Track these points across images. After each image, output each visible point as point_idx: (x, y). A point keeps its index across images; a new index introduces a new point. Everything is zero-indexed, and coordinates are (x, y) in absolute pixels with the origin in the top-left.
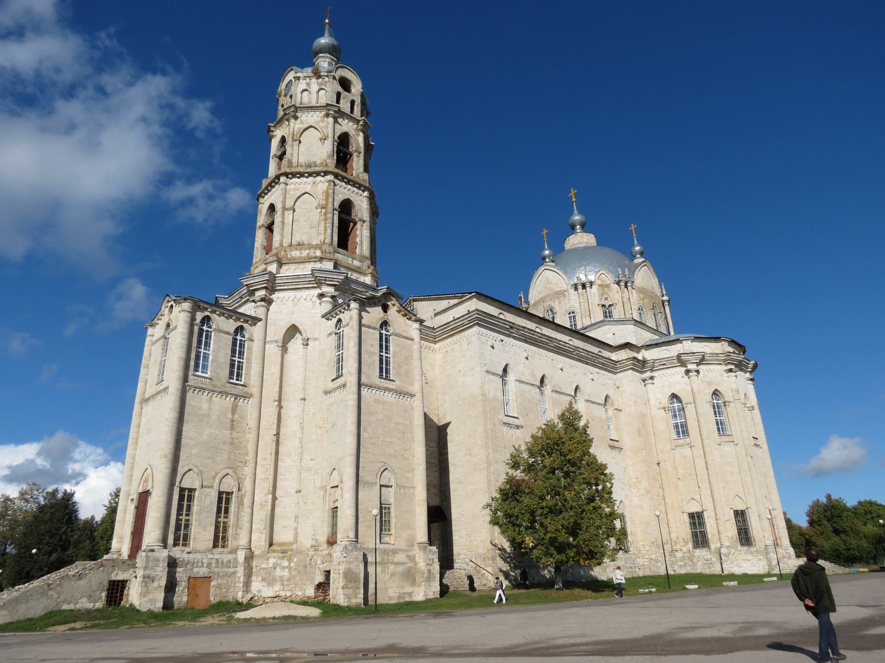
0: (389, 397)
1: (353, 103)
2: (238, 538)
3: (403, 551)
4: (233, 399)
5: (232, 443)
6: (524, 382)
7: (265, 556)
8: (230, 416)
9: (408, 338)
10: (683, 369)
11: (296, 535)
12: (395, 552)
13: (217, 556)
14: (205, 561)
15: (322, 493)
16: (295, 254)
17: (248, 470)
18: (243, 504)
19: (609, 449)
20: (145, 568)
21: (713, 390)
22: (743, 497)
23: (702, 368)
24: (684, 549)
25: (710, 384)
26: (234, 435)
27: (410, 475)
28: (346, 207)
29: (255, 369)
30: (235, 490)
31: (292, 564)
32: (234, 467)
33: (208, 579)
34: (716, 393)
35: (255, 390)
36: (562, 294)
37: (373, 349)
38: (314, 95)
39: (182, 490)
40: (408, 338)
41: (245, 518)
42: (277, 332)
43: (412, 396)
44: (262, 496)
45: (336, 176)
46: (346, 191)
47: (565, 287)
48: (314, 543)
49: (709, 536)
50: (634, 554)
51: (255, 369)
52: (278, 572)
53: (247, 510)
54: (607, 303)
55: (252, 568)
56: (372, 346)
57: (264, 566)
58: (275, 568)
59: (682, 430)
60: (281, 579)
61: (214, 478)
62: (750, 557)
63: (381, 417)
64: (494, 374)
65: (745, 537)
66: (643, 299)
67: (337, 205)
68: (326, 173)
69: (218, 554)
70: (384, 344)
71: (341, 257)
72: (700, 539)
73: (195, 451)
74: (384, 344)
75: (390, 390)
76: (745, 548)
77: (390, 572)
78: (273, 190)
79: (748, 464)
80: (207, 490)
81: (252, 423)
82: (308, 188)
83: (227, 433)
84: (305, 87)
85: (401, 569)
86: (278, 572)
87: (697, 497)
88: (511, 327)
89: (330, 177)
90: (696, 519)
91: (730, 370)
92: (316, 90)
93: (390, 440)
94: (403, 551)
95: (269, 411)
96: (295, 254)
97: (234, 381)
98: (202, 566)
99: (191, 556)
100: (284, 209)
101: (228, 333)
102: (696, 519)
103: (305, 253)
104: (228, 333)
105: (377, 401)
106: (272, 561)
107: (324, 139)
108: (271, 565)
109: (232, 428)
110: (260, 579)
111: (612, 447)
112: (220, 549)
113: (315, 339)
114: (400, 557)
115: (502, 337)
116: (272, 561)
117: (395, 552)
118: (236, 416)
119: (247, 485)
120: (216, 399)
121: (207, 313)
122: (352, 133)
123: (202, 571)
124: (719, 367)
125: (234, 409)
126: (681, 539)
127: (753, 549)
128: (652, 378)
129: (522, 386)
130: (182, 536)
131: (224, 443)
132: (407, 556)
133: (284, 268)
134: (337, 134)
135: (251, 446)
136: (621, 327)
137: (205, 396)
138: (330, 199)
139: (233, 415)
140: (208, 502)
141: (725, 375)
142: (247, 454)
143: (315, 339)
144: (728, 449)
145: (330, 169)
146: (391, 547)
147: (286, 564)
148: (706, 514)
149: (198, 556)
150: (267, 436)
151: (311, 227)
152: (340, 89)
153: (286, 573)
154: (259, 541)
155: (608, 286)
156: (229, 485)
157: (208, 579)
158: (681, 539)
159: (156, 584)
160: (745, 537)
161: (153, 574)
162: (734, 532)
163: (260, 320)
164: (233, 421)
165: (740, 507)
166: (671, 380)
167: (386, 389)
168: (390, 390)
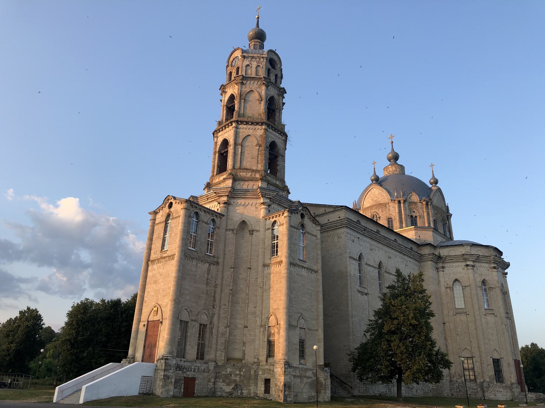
0: (304, 272)
1: (276, 76)
2: (210, 355)
4: (208, 265)
5: (207, 293)
7: (224, 366)
8: (206, 276)
11: (244, 354)
13: (199, 365)
14: (193, 367)
15: (262, 330)
18: (212, 333)
20: (165, 370)
22: (499, 351)
23: (477, 264)
24: (459, 381)
25: (481, 275)
26: (208, 288)
27: (314, 322)
30: (208, 323)
31: (242, 373)
33: (194, 379)
34: (484, 282)
35: (221, 261)
36: (383, 206)
41: (214, 342)
43: (316, 272)
45: (268, 125)
48: (256, 360)
51: (221, 246)
52: (233, 377)
53: (215, 337)
56: (296, 240)
57: (224, 373)
58: (231, 375)
60: (235, 380)
61: (197, 315)
62: (502, 390)
66: (436, 214)
69: (198, 364)
73: (188, 298)
76: (499, 384)
77: (304, 382)
78: (227, 129)
80: (194, 323)
82: (251, 132)
83: (204, 286)
84: (248, 64)
85: (310, 380)
86: (233, 377)
87: (469, 348)
88: (365, 230)
92: (255, 66)
93: (304, 299)
94: (311, 370)
95: (228, 273)
97: (208, 254)
98: (191, 371)
99: (186, 364)
100: (236, 144)
103: (249, 175)
105: (298, 274)
108: (228, 372)
109: (207, 284)
110: (221, 381)
113: (257, 231)
114: (309, 374)
115: (358, 235)
116: (229, 370)
118: (209, 276)
121: (196, 211)
122: (276, 97)
123: (190, 374)
124: (487, 265)
126: (457, 374)
127: (504, 385)
128: (443, 267)
132: (313, 373)
134: (268, 97)
139: (208, 275)
140: (194, 330)
142: (214, 301)
143: (257, 231)
146: (305, 367)
147: (238, 372)
149: (189, 364)
151: (252, 158)
152: (270, 67)
153: (238, 378)
154: (221, 357)
156: (204, 319)
157: (194, 379)
158: (457, 374)
159: (169, 381)
162: (492, 373)
163: (223, 215)
164: (207, 279)
165: (496, 357)
168: (305, 268)
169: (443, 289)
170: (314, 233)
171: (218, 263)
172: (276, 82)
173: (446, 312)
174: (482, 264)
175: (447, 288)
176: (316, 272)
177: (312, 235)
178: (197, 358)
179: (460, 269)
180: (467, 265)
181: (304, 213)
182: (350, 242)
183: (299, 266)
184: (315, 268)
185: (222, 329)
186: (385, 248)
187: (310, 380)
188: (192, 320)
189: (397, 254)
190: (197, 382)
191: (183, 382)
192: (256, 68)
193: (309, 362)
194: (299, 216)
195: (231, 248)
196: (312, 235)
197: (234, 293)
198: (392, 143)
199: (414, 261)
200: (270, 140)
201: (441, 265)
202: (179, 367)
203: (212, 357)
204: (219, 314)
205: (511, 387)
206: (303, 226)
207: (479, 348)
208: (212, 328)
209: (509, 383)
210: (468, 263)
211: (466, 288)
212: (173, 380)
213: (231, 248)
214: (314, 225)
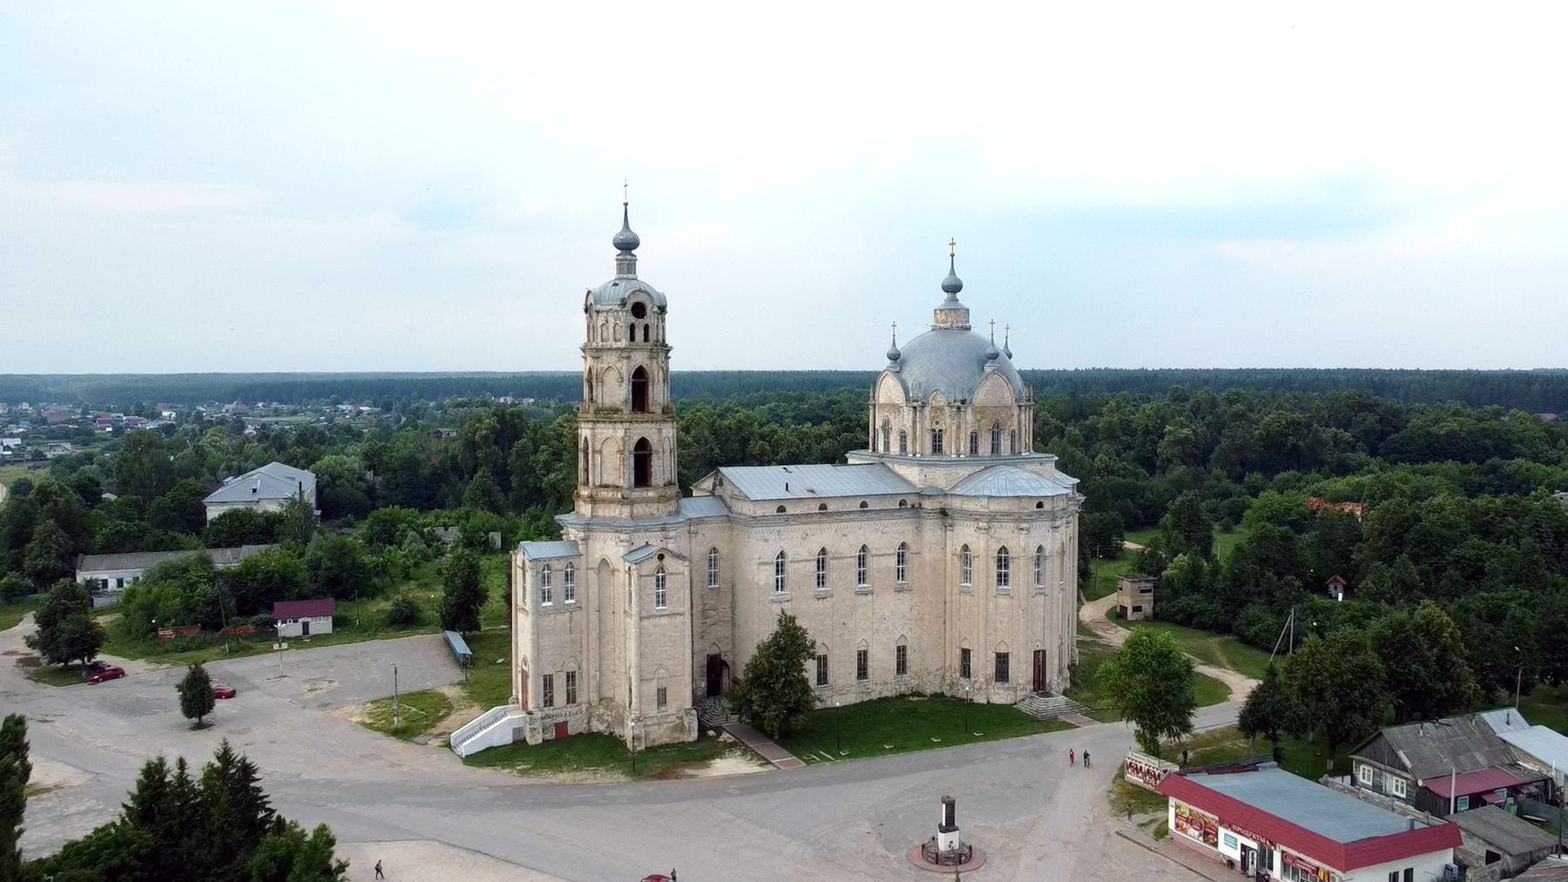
1: (646, 328)
2: (582, 698)
17: (584, 656)
25: (999, 540)
28: (643, 444)
29: (583, 590)
51: (583, 590)
54: (938, 428)
59: (967, 576)
65: (1002, 673)
67: (632, 448)
70: (661, 582)
71: (639, 493)
72: (966, 671)
74: (661, 582)
90: (966, 654)
95: (594, 617)
102: (966, 654)
119: (584, 666)
123: (561, 720)
125: (571, 619)
130: (549, 702)
144: (1003, 601)
150: (594, 635)
152: (633, 319)
154: (594, 697)
155: (941, 409)
156: (572, 667)
160: (1002, 673)
166: (966, 533)
169: (949, 556)
179: (971, 530)
185: (592, 672)
195: (594, 588)
197: (600, 637)
200: (636, 439)
205: (1015, 690)
206: (661, 569)
213: (594, 588)
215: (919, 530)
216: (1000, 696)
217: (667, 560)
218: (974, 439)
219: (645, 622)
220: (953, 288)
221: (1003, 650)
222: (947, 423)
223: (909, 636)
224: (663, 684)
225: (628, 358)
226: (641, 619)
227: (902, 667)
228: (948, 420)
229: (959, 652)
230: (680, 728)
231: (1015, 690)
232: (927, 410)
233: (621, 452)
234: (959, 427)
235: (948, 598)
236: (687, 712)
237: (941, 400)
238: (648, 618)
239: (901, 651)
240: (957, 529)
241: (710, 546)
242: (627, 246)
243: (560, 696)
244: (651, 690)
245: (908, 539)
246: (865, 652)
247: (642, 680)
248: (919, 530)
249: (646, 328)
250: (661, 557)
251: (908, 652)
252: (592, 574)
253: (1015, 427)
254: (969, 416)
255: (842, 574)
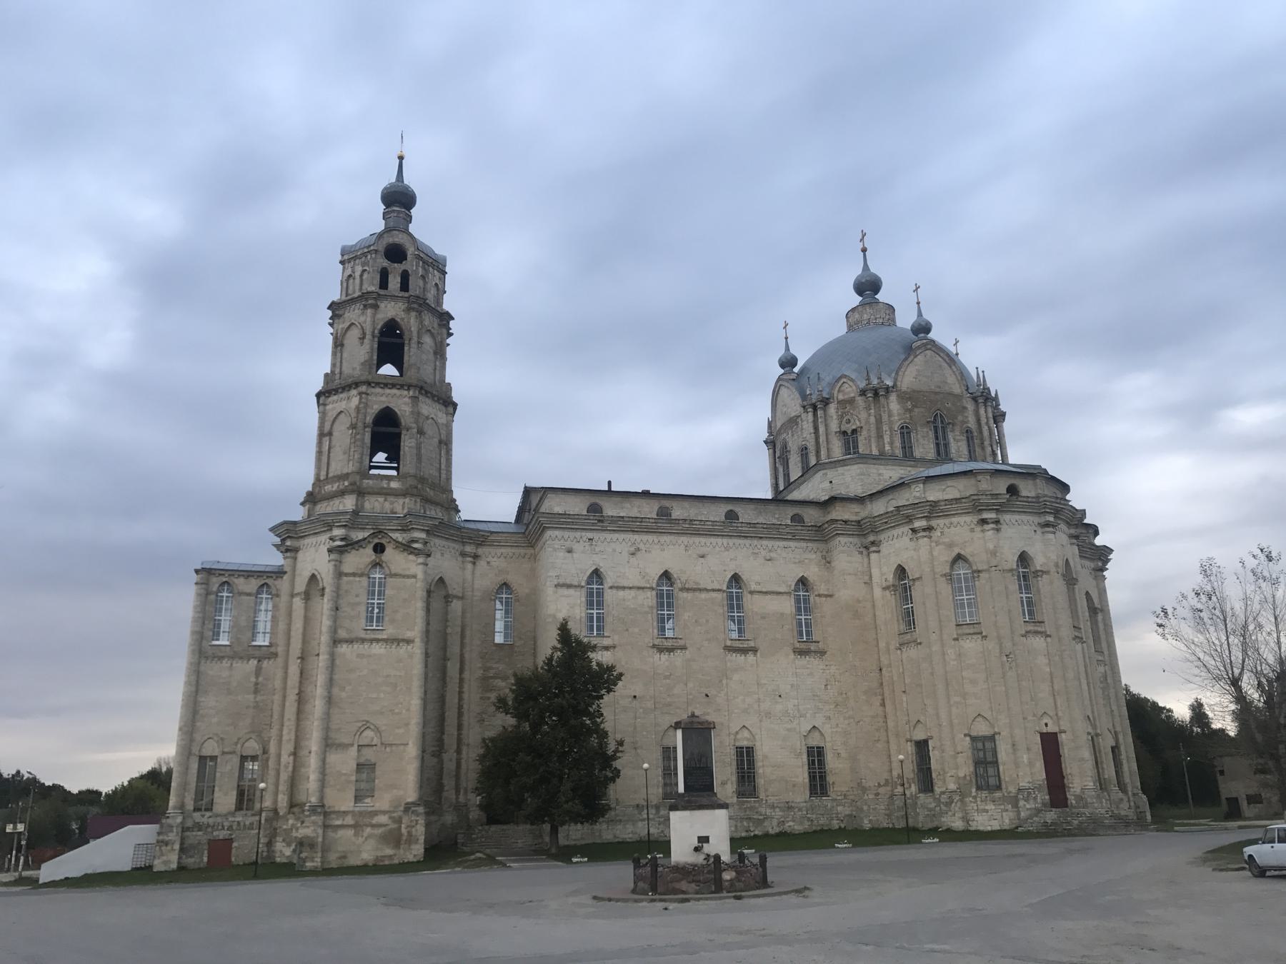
0: (378, 649)
1: (405, 277)
3: (384, 812)
6: (624, 588)
8: (253, 679)
9: (408, 577)
10: (906, 529)
12: (376, 813)
13: (240, 819)
14: (226, 824)
16: (328, 488)
17: (274, 732)
19: (792, 656)
21: (954, 554)
25: (950, 546)
27: (401, 731)
32: (258, 732)
33: (229, 841)
35: (280, 650)
36: (793, 422)
37: (357, 600)
38: (358, 281)
39: (202, 759)
40: (408, 577)
42: (301, 586)
43: (408, 641)
44: (286, 759)
46: (383, 399)
47: (797, 413)
49: (934, 775)
50: (834, 800)
54: (849, 428)
55: (275, 829)
59: (909, 618)
61: (236, 744)
62: (990, 807)
63: (365, 672)
64: (569, 586)
66: (910, 411)
67: (369, 419)
68: (357, 384)
72: (926, 780)
73: (215, 720)
75: (378, 640)
77: (365, 834)
79: (1003, 665)
81: (278, 684)
82: (342, 405)
83: (251, 697)
85: (381, 830)
89: (363, 388)
91: (984, 522)
94: (384, 812)
95: (294, 669)
96: (328, 488)
101: (249, 594)
104: (249, 594)
105: (360, 656)
106: (291, 822)
107: (362, 338)
109: (256, 692)
111: (801, 653)
112: (243, 812)
114: (383, 819)
115: (590, 535)
117: (376, 813)
118: (260, 679)
120: (238, 665)
123: (222, 834)
124: (968, 519)
125: (258, 672)
127: (998, 794)
129: (621, 593)
131: (248, 707)
133: (318, 507)
135: (276, 708)
136: (840, 470)
137: (226, 663)
138: (360, 416)
139: (257, 675)
140: (229, 767)
141: (978, 529)
145: (363, 378)
148: (931, 743)
149: (219, 820)
152: (386, 263)
154: (283, 801)
155: (851, 401)
157: (229, 841)
161: (166, 838)
164: (256, 684)
167: (372, 641)
168: (378, 640)
169: (878, 592)
170: (411, 572)
171: (275, 655)
172: (405, 286)
173: (882, 645)
174: (955, 520)
175: (884, 589)
176: (409, 641)
177: (404, 576)
178: (239, 807)
180: (914, 530)
181: (376, 541)
182: (562, 554)
183: (363, 641)
184: (409, 635)
186: (684, 539)
187: (381, 830)
188: (224, 753)
189: (731, 541)
190: (235, 844)
191: (206, 847)
192: (361, 276)
193: (382, 802)
194: (369, 551)
196: (404, 576)
198: (864, 250)
199: (803, 544)
200: (376, 408)
201: (871, 538)
202: (199, 826)
203: (268, 803)
204: (281, 736)
205: (1015, 802)
207: (937, 715)
208: (267, 760)
209: (1013, 790)
210: (917, 524)
211: (917, 583)
212: (177, 847)
214: (412, 557)
215: (827, 562)
216: (989, 816)
217: (390, 554)
218: (905, 432)
219: (343, 649)
220: (868, 287)
221: (982, 729)
222: (862, 416)
223: (826, 729)
224: (369, 755)
225: (376, 307)
226: (336, 642)
227: (818, 782)
228: (863, 415)
229: (910, 748)
230: (394, 838)
231: (1015, 802)
232: (832, 409)
233: (353, 426)
234: (879, 422)
235: (884, 660)
236: (408, 808)
237: (850, 391)
238: (350, 641)
239: (816, 757)
240: (885, 548)
241: (500, 579)
242: (399, 200)
243: (225, 800)
244: (344, 762)
245: (813, 572)
246: (750, 751)
247: (328, 744)
248: (827, 562)
249: (405, 277)
250: (379, 549)
251: (829, 758)
252: (298, 603)
253: (972, 424)
254: (894, 404)
255: (701, 621)
